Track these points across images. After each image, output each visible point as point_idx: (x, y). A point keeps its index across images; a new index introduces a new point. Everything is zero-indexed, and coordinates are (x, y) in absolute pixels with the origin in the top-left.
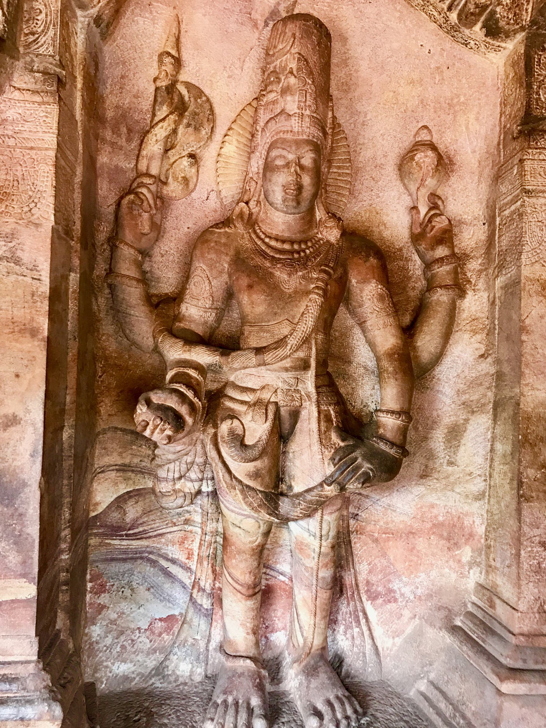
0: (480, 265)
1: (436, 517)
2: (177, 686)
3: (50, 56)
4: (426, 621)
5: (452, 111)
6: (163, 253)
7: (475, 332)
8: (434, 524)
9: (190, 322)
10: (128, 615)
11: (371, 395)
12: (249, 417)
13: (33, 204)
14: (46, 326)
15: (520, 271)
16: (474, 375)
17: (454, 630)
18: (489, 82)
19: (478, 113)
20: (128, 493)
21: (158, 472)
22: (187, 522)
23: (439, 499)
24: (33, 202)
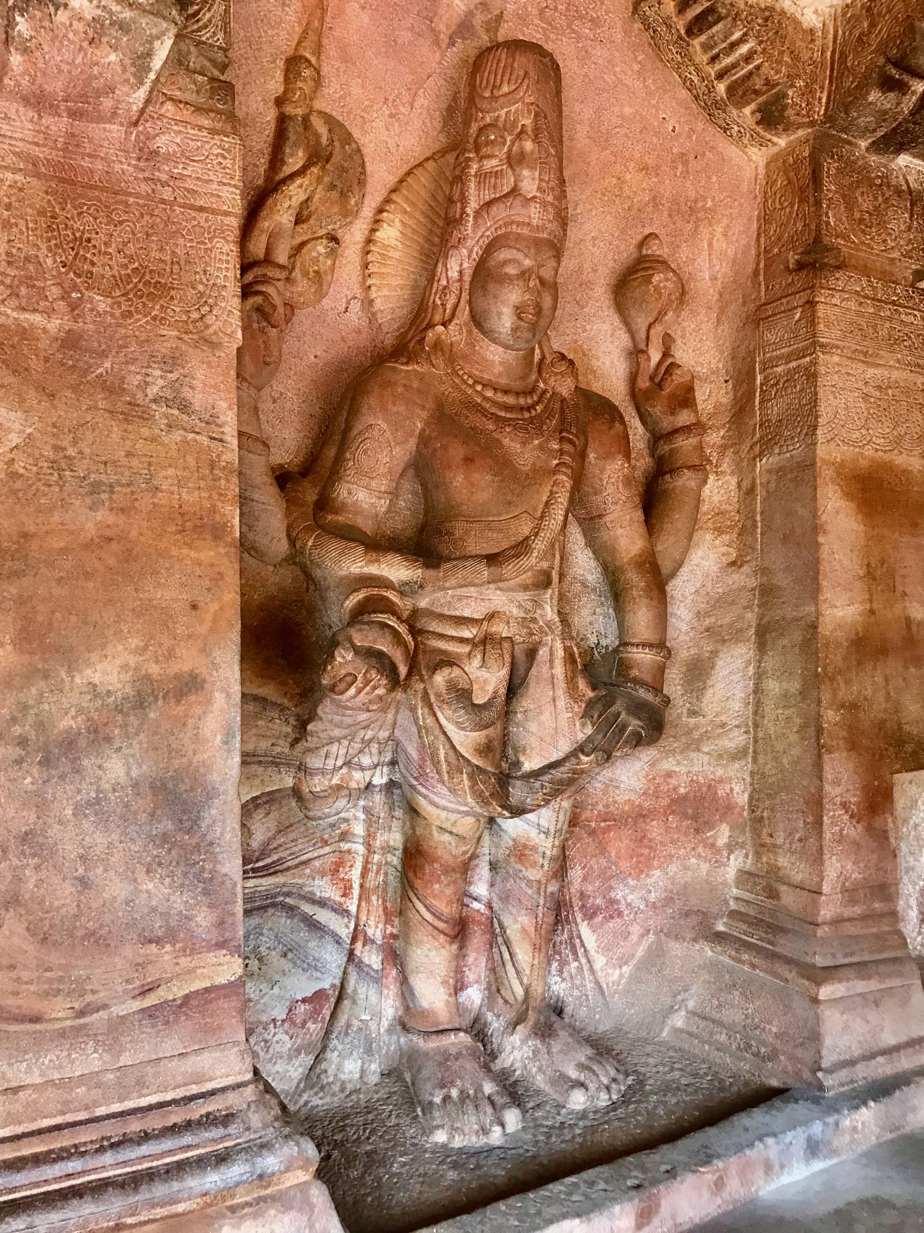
0: (723, 437)
1: (675, 789)
3: (220, 48)
5: (693, 218)
7: (719, 531)
8: (672, 800)
9: (356, 513)
11: (591, 623)
12: (477, 661)
14: (236, 521)
15: (814, 451)
16: (720, 590)
17: (719, 938)
18: (745, 187)
19: (728, 226)
21: (308, 760)
22: (344, 836)
23: (679, 764)
24: (205, 301)
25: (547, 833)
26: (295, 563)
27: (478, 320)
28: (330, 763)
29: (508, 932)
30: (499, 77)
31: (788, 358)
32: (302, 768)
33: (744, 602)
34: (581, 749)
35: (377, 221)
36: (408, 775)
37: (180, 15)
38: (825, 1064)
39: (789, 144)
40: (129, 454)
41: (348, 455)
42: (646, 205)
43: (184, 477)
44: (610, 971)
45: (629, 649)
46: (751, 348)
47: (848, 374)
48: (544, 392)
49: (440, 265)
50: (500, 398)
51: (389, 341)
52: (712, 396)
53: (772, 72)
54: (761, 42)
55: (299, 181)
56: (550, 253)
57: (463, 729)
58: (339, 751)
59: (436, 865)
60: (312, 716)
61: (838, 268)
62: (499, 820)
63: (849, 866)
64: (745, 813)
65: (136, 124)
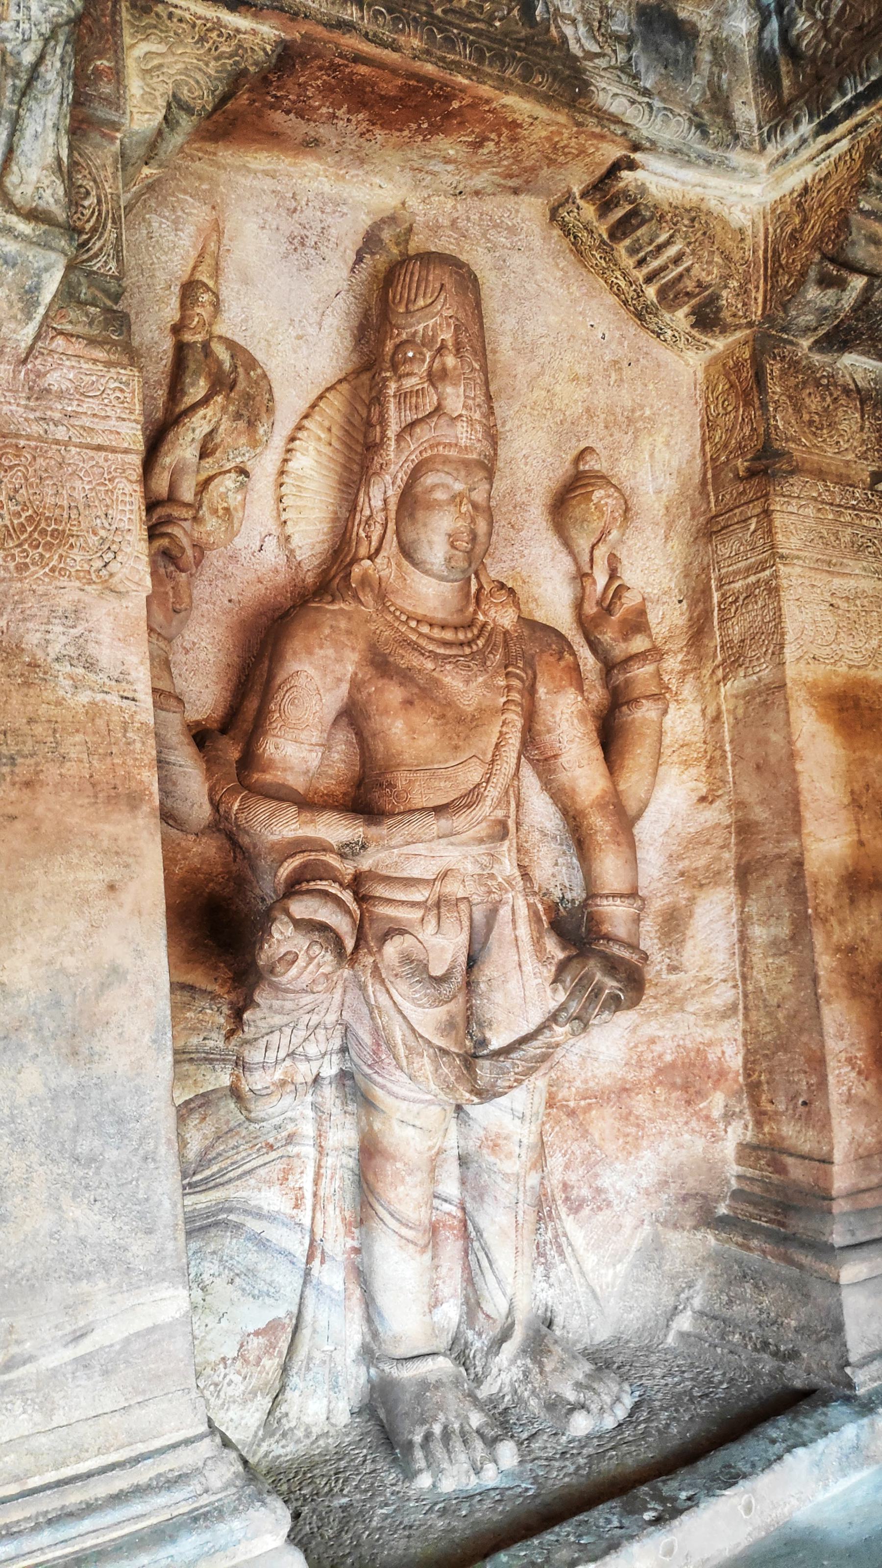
0: (681, 662)
2: (313, 1443)
4: (664, 1224)
5: (631, 430)
6: (188, 646)
7: (686, 764)
9: (284, 770)
10: (203, 1339)
11: (554, 875)
13: (111, 555)
14: (155, 788)
16: (692, 830)
20: (187, 1103)
21: (246, 1053)
22: (290, 1139)
24: (109, 549)
25: (523, 1118)
26: (219, 830)
27: (407, 551)
28: (272, 1056)
29: (485, 1235)
30: (413, 291)
31: (748, 571)
32: (240, 1063)
33: (720, 842)
34: (554, 1018)
35: (289, 451)
36: (360, 1062)
37: (70, 245)
38: (853, 1357)
39: (728, 347)
40: (31, 721)
41: (273, 706)
42: (579, 418)
43: (93, 743)
44: (603, 1271)
45: (598, 901)
46: (705, 563)
47: (813, 586)
48: (485, 625)
49: (362, 494)
50: (436, 633)
51: (310, 579)
52: (668, 618)
53: (704, 274)
54: (689, 243)
55: (201, 412)
56: (482, 474)
57: (420, 1006)
58: (281, 1042)
59: (398, 1165)
60: (249, 1002)
61: (792, 473)
62: (467, 1108)
63: (861, 1129)
64: (741, 1079)
65: (24, 362)
